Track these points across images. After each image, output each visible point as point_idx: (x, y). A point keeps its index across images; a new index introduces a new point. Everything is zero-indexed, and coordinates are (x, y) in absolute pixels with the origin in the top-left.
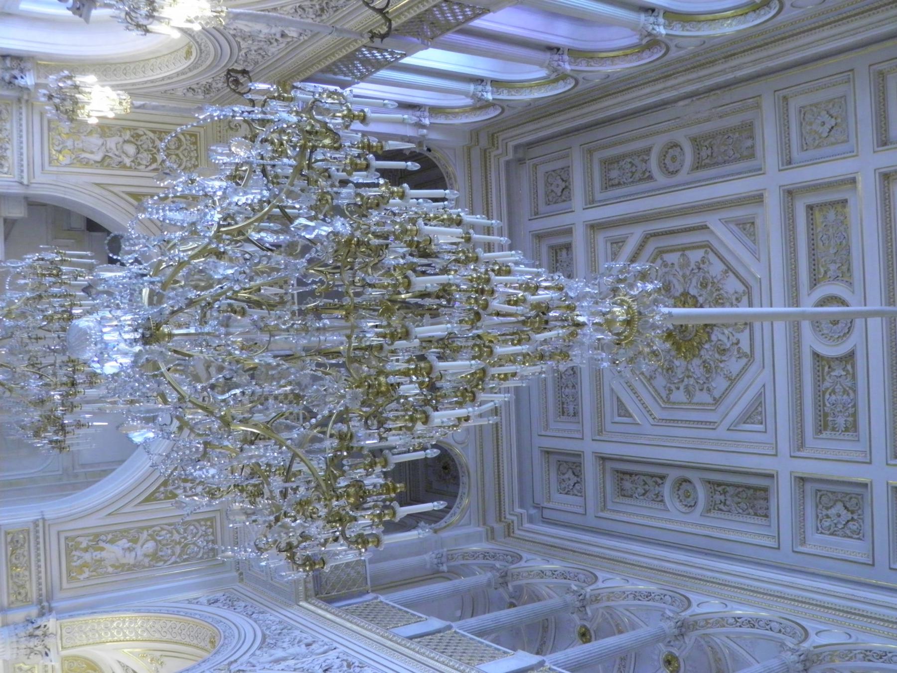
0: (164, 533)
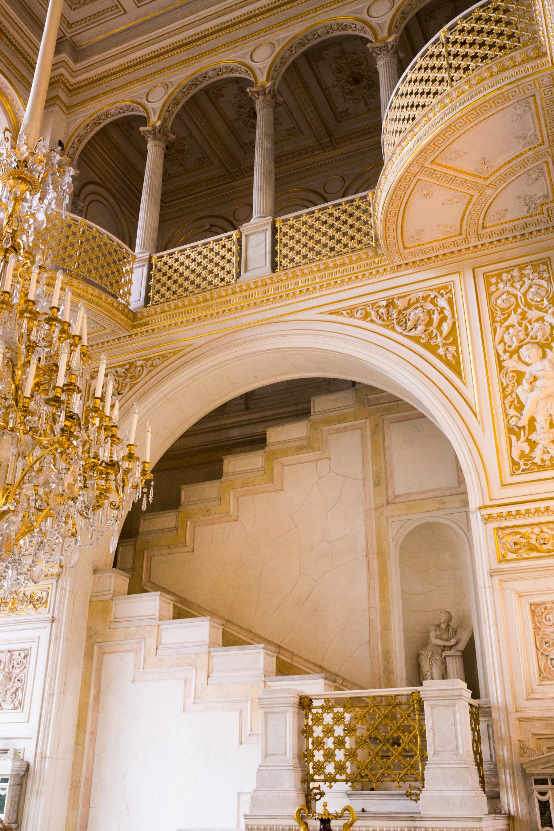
0: (506, 337)
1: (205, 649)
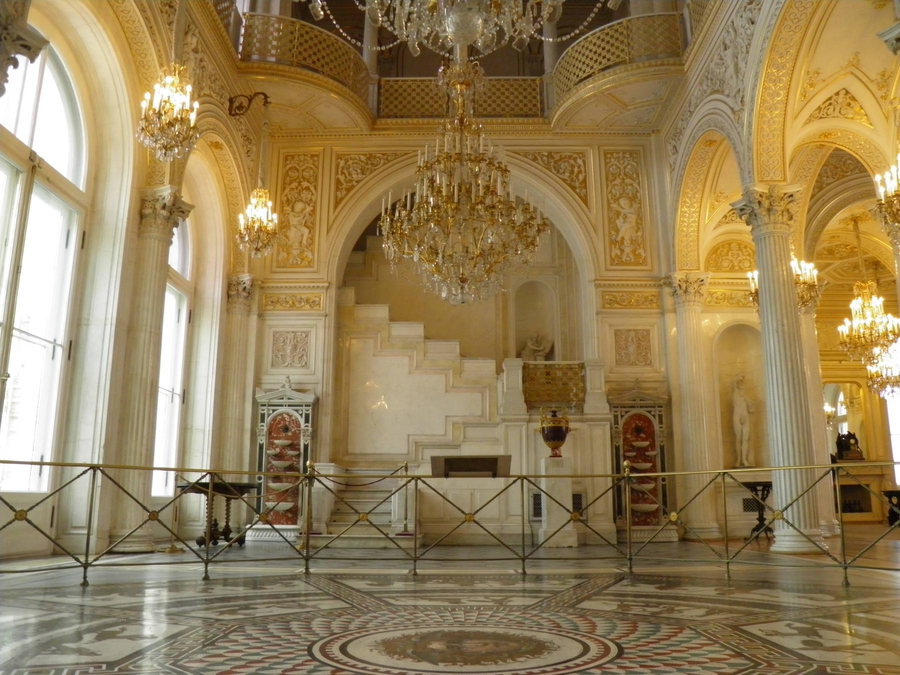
0: (613, 192)
1: (422, 340)
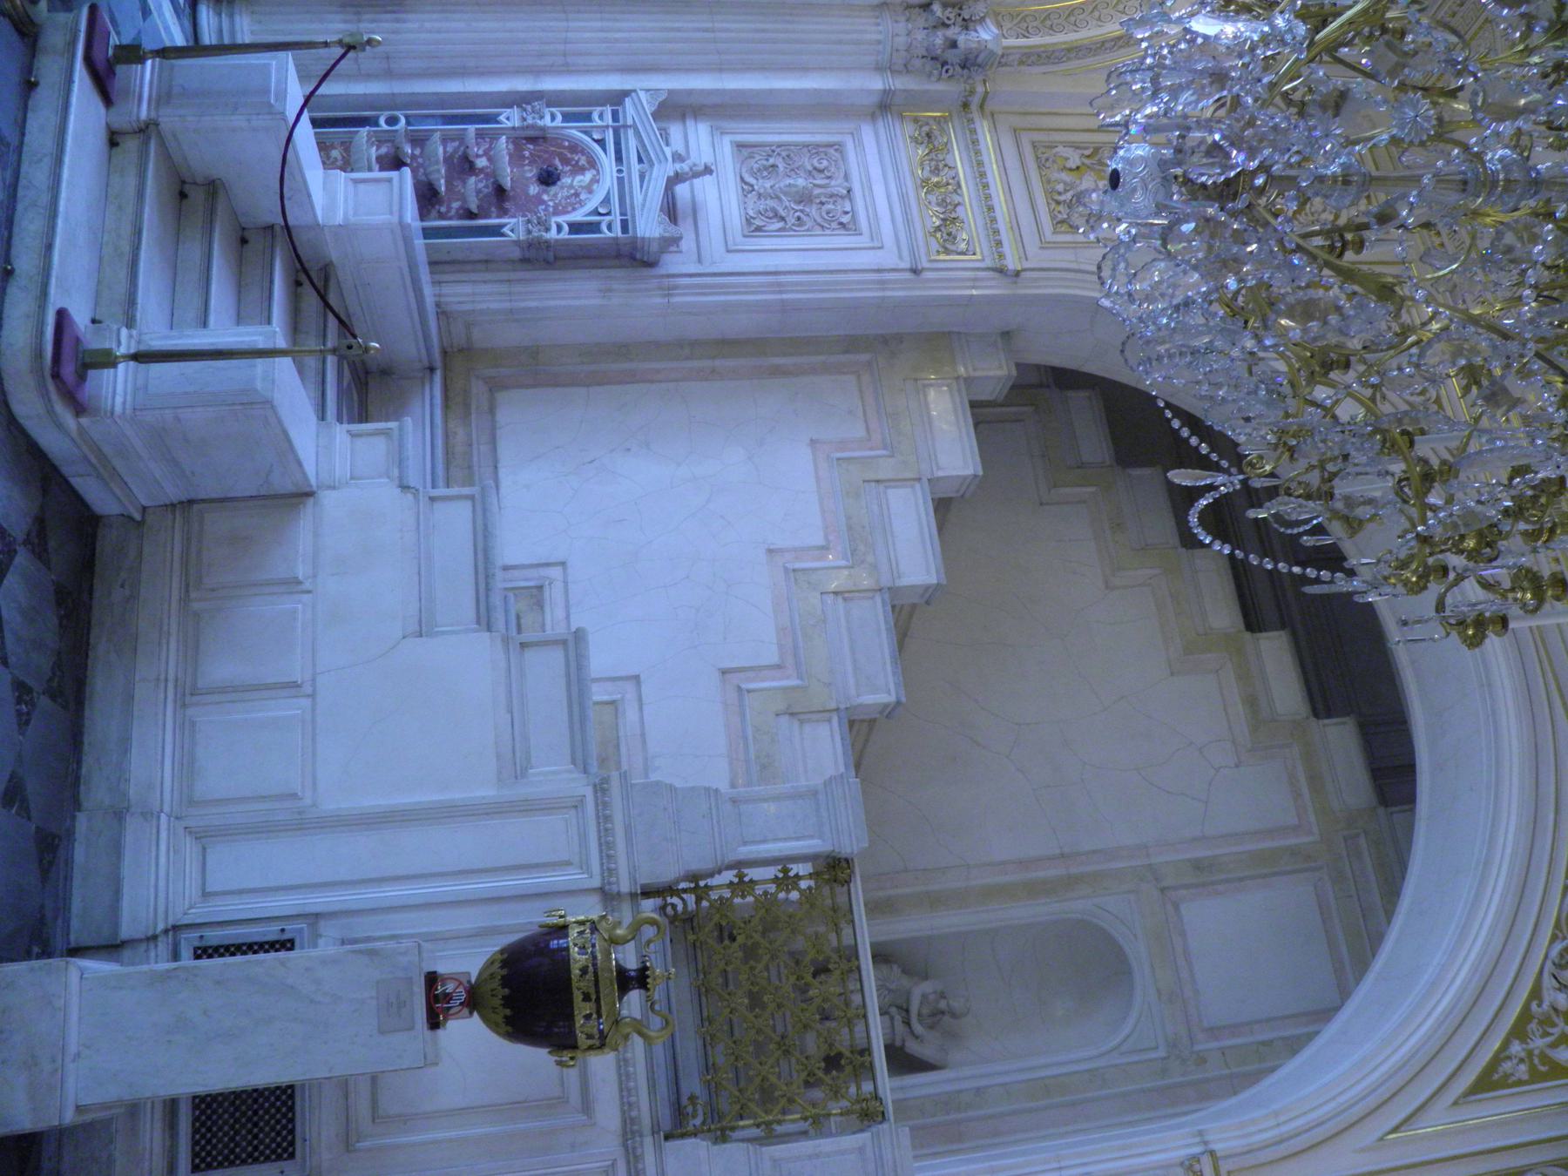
1: (886, 582)
